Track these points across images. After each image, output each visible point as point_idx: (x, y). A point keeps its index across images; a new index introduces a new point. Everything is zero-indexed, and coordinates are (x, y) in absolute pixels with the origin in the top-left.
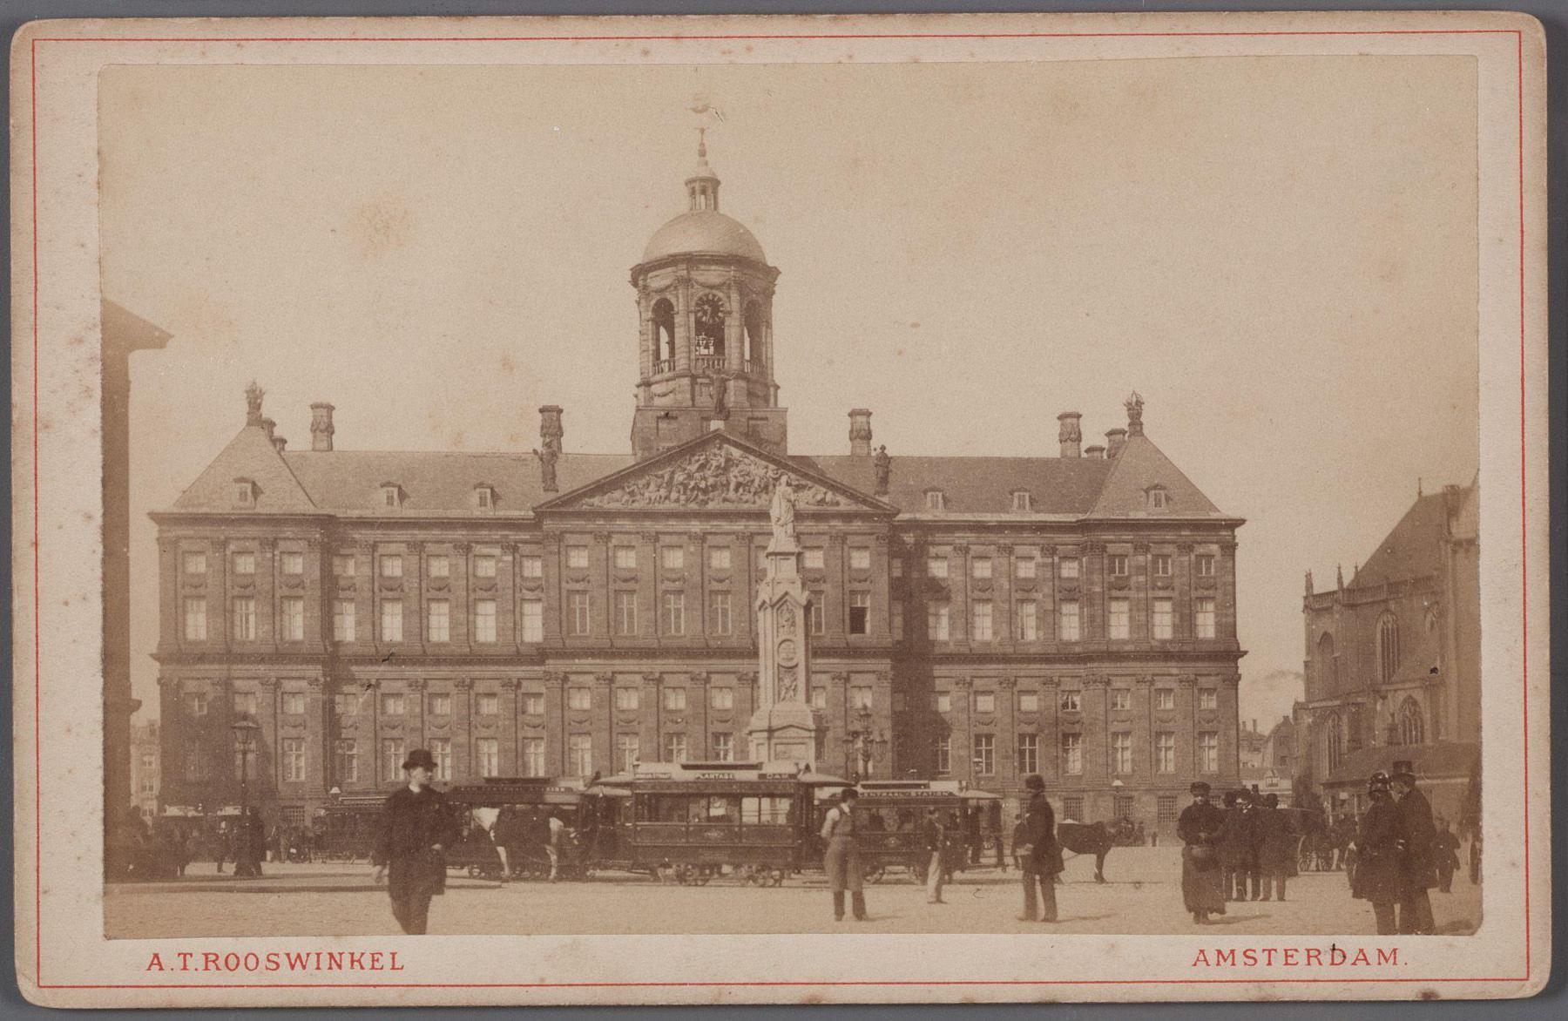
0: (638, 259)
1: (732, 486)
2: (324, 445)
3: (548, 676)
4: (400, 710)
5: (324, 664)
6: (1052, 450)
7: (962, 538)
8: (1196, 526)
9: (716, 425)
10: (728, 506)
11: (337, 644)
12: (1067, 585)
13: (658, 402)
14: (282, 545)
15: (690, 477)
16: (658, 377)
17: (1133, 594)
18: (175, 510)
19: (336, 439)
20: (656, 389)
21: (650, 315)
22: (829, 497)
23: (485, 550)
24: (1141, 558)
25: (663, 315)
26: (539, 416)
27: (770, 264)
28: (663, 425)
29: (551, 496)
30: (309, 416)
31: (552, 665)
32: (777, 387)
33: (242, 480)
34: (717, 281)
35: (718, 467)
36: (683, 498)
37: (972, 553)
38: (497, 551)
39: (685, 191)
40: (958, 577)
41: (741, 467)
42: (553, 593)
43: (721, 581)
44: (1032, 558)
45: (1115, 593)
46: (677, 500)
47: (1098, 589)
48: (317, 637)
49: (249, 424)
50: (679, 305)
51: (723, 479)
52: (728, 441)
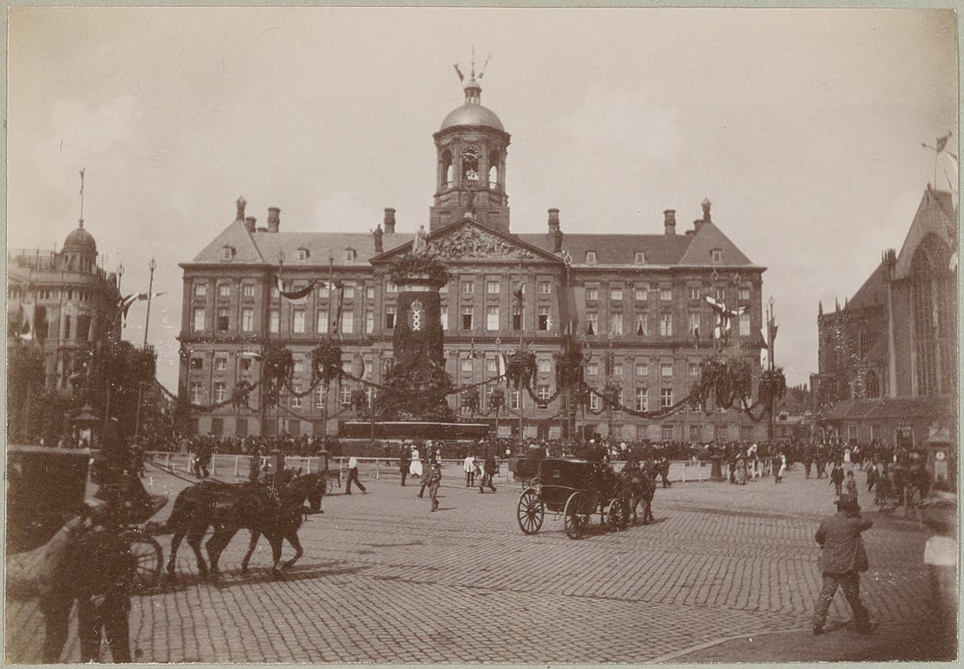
0: (438, 131)
1: (475, 248)
2: (274, 229)
3: (373, 352)
4: (301, 369)
5: (262, 343)
6: (660, 230)
7: (604, 278)
8: (740, 271)
9: (468, 215)
10: (471, 259)
11: (268, 333)
12: (664, 304)
13: (444, 205)
14: (244, 281)
15: (452, 244)
16: (443, 192)
17: (701, 309)
18: (193, 262)
19: (280, 226)
20: (443, 198)
21: (441, 159)
22: (528, 253)
23: (348, 284)
24: (706, 289)
25: (446, 159)
26: (384, 213)
27: (506, 131)
28: (443, 217)
29: (380, 253)
30: (266, 215)
31: (375, 346)
32: (507, 197)
33: (226, 247)
34: (475, 139)
35: (467, 238)
36: (448, 254)
37: (611, 286)
38: (354, 284)
39: (464, 94)
40: (603, 300)
41: (482, 238)
42: (378, 305)
43: (468, 300)
44: (644, 289)
45: (692, 309)
46: (445, 256)
47: (681, 307)
48: (259, 329)
49: (237, 219)
50: (455, 153)
51: (470, 244)
52: (478, 226)
